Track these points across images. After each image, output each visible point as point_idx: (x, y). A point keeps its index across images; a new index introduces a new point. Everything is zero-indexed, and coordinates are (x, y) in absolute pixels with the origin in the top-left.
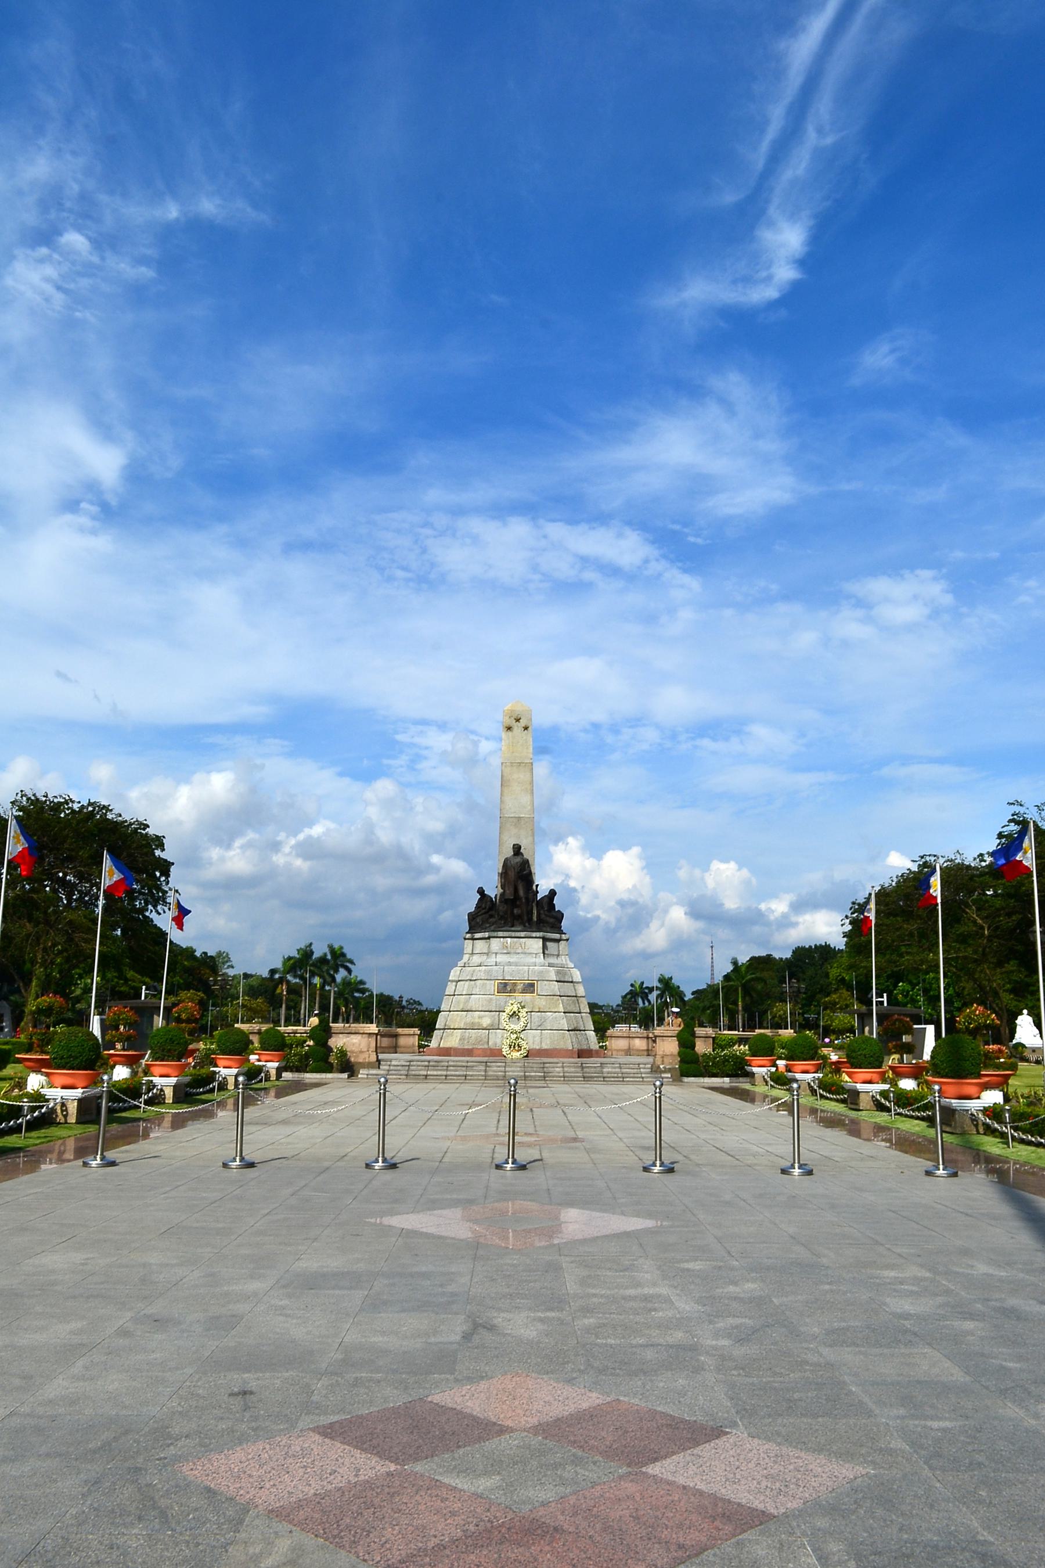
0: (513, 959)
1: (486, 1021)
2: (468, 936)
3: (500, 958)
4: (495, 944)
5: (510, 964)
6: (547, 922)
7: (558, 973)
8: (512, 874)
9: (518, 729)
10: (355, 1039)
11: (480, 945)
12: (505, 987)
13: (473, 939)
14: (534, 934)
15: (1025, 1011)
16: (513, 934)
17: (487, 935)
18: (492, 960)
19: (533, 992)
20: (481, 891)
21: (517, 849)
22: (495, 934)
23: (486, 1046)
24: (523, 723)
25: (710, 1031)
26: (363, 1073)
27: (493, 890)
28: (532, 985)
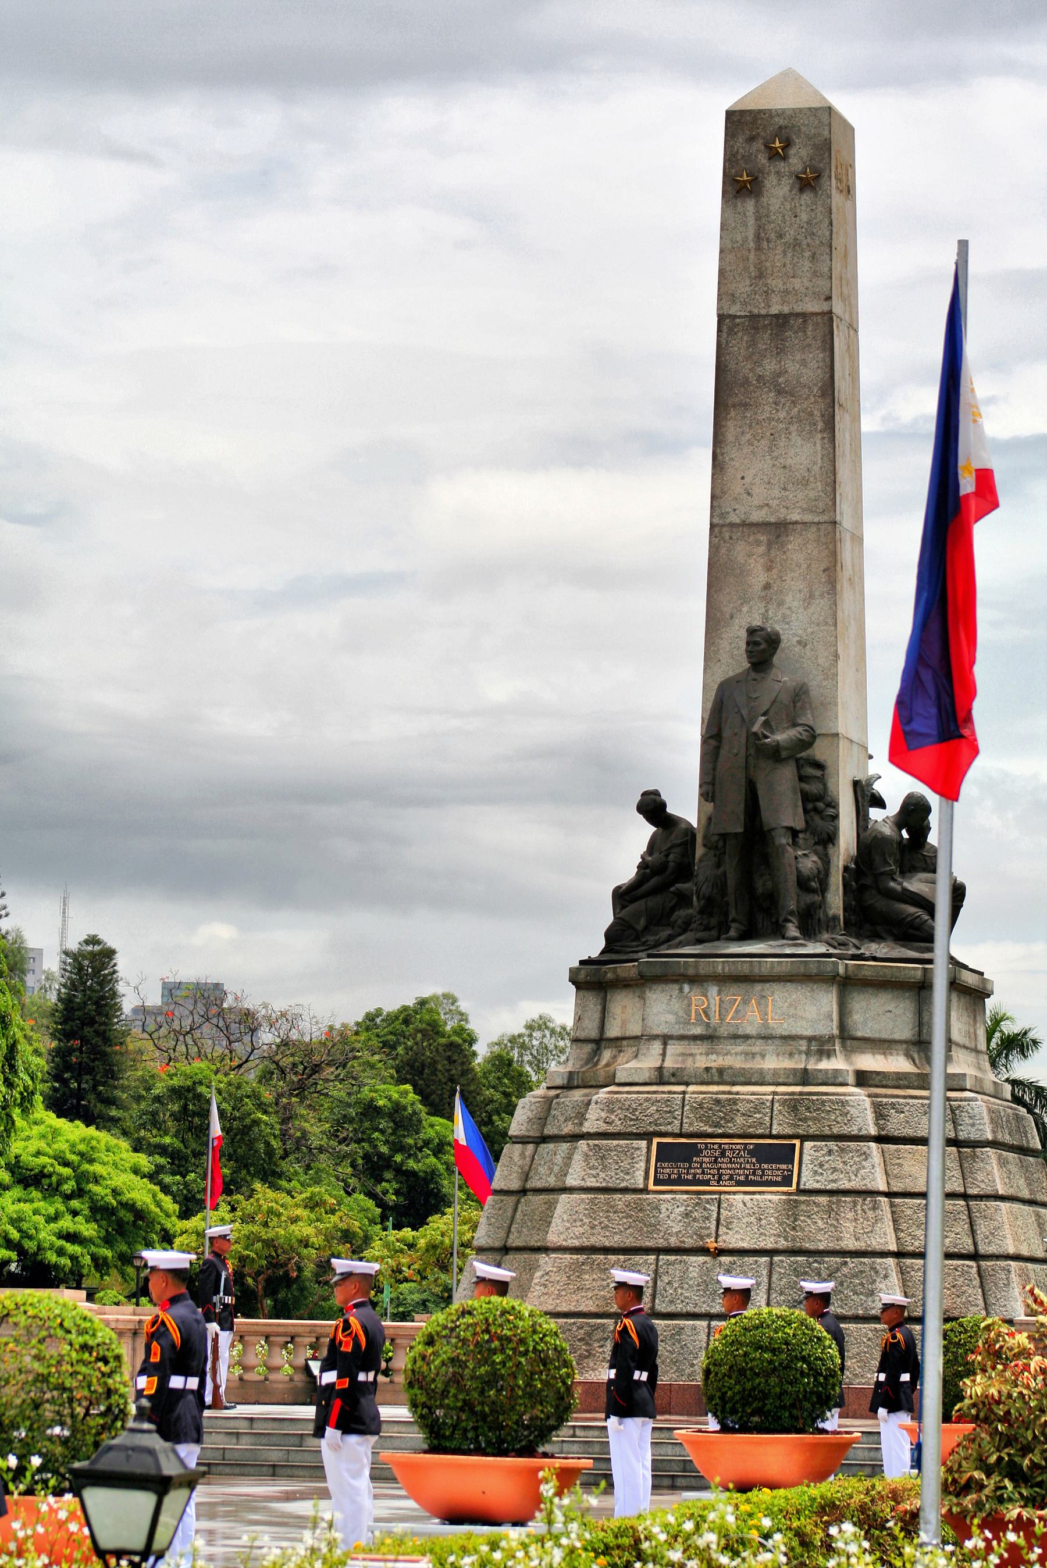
8: (735, 745)
19: (787, 1181)
20: (652, 808)
24: (798, 158)
27: (686, 806)
28: (786, 1154)
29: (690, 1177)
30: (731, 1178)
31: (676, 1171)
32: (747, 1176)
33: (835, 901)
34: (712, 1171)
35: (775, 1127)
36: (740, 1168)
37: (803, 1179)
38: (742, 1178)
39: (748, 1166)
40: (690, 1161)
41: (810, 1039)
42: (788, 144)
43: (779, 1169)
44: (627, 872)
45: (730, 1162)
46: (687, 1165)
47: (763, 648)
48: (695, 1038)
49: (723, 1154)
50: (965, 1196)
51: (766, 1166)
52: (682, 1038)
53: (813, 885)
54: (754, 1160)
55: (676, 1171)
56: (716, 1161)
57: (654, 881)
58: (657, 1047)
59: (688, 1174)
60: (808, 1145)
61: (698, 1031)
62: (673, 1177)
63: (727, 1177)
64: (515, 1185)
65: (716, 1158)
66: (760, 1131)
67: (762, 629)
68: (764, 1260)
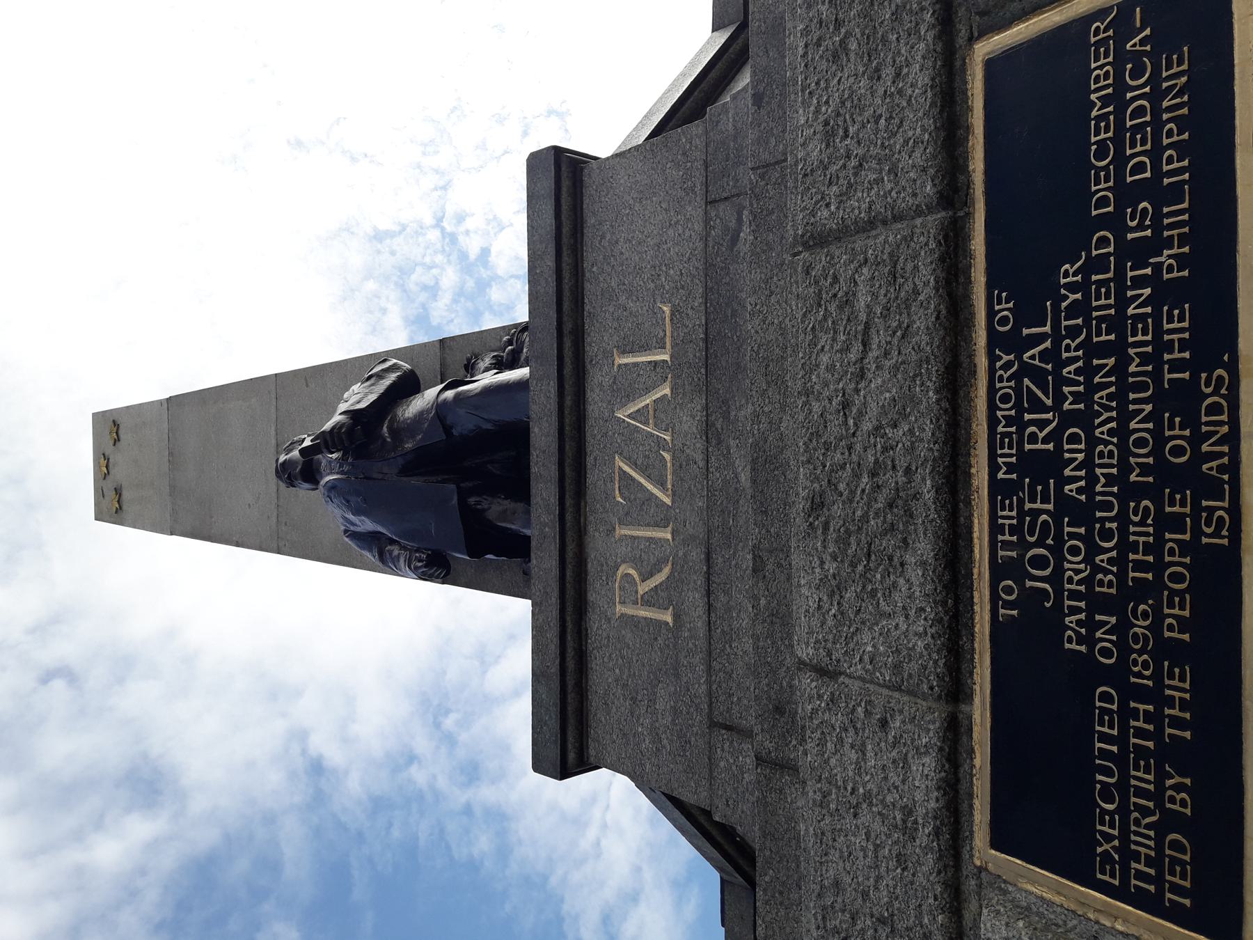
29: (1178, 688)
30: (1180, 402)
31: (1142, 778)
32: (1165, 294)
34: (1141, 534)
35: (906, 201)
36: (1119, 349)
38: (1177, 326)
39: (1104, 304)
40: (1088, 671)
43: (1117, 99)
45: (1085, 419)
46: (1105, 697)
49: (1041, 468)
51: (1101, 189)
54: (1069, 273)
55: (1142, 778)
56: (1082, 513)
59: (1156, 696)
62: (1181, 804)
63: (1178, 435)
65: (1065, 506)
66: (925, 276)
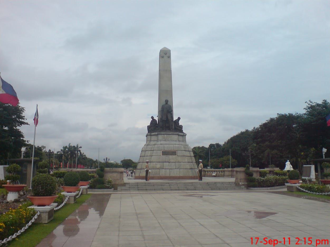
0: (167, 142)
1: (158, 166)
2: (149, 134)
3: (162, 142)
4: (160, 137)
5: (166, 144)
6: (178, 129)
7: (184, 147)
9: (166, 57)
10: (115, 175)
11: (153, 138)
12: (165, 153)
13: (151, 135)
14: (175, 133)
15: (288, 161)
16: (167, 133)
17: (156, 133)
18: (159, 143)
20: (152, 118)
21: (167, 102)
22: (160, 133)
23: (159, 176)
25: (258, 169)
26: (119, 188)
33: (173, 127)
37: (178, 155)
41: (176, 141)
42: (167, 53)
44: (149, 125)
47: (167, 102)
48: (164, 140)
50: (190, 156)
52: (163, 140)
53: (172, 126)
57: (154, 125)
58: (160, 141)
60: (178, 151)
61: (164, 140)
64: (144, 156)
67: (167, 100)
68: (174, 163)
